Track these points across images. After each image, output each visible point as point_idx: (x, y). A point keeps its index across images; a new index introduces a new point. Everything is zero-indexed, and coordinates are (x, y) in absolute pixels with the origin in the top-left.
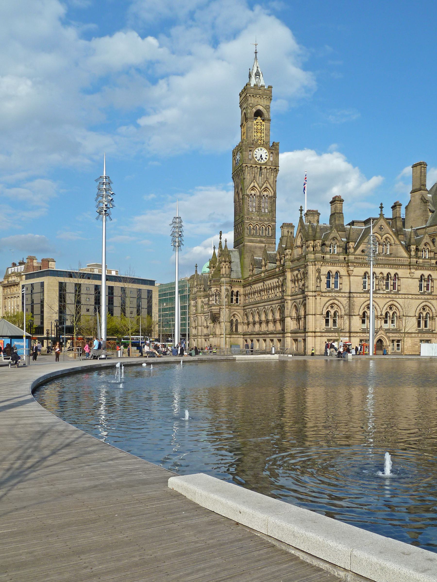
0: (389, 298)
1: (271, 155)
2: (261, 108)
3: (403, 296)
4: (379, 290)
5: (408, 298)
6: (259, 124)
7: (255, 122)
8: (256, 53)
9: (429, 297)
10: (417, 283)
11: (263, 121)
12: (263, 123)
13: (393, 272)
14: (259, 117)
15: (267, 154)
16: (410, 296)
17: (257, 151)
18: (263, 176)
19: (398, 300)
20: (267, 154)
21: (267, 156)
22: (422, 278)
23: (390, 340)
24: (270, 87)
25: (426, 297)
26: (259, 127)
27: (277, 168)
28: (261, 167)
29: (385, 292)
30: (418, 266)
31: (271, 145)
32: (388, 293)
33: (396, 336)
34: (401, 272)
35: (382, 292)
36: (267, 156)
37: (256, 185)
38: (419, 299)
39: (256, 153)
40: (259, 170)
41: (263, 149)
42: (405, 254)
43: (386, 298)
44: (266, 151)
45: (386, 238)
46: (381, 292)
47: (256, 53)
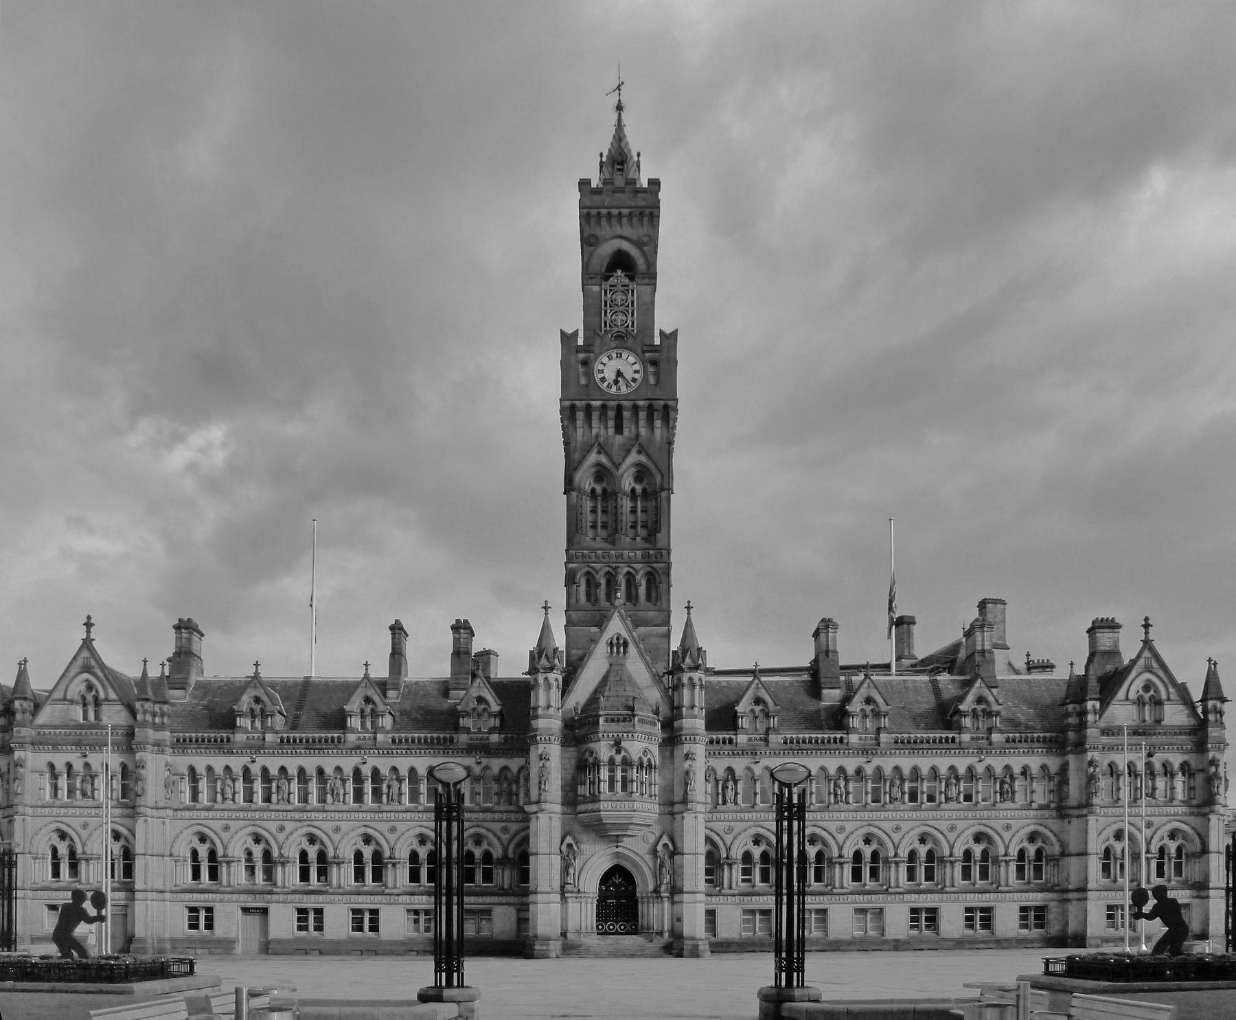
1: (651, 369)
2: (625, 246)
6: (619, 287)
7: (605, 285)
8: (619, 108)
11: (632, 278)
12: (633, 285)
14: (619, 272)
15: (637, 367)
17: (605, 360)
18: (626, 432)
21: (636, 372)
26: (619, 297)
27: (671, 403)
28: (619, 409)
31: (657, 341)
36: (636, 372)
37: (604, 460)
39: (601, 367)
40: (611, 414)
44: (632, 359)
47: (619, 108)
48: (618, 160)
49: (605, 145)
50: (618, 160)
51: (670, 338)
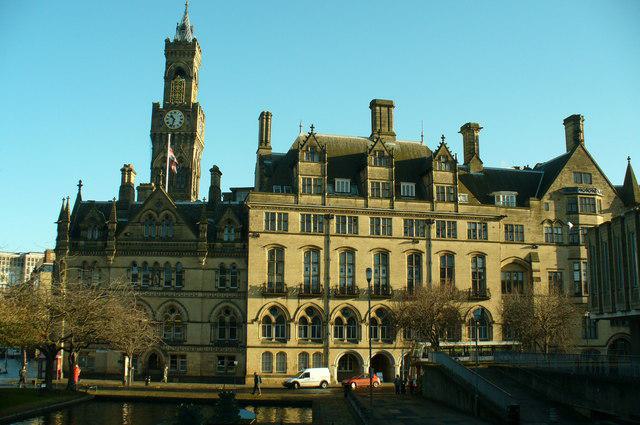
0: (167, 296)
3: (189, 294)
4: (153, 285)
5: (196, 297)
9: (233, 295)
10: (211, 275)
13: (173, 261)
16: (200, 295)
19: (181, 300)
20: (183, 117)
22: (222, 270)
23: (166, 356)
24: (195, 40)
25: (227, 295)
29: (160, 289)
30: (213, 253)
32: (165, 290)
33: (177, 350)
34: (185, 261)
35: (156, 288)
38: (215, 297)
41: (177, 111)
42: (192, 236)
43: (162, 296)
45: (167, 216)
46: (156, 288)
48: (182, 29)
49: (180, 21)
50: (182, 29)
51: (196, 105)
